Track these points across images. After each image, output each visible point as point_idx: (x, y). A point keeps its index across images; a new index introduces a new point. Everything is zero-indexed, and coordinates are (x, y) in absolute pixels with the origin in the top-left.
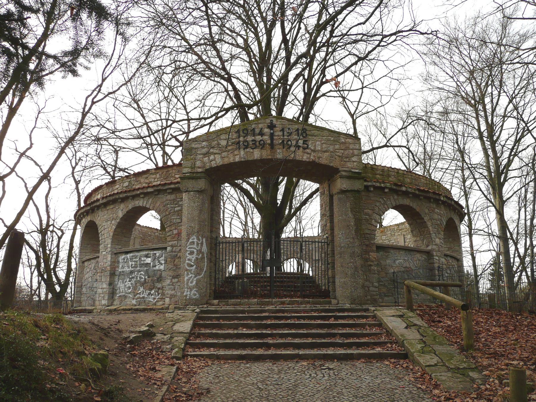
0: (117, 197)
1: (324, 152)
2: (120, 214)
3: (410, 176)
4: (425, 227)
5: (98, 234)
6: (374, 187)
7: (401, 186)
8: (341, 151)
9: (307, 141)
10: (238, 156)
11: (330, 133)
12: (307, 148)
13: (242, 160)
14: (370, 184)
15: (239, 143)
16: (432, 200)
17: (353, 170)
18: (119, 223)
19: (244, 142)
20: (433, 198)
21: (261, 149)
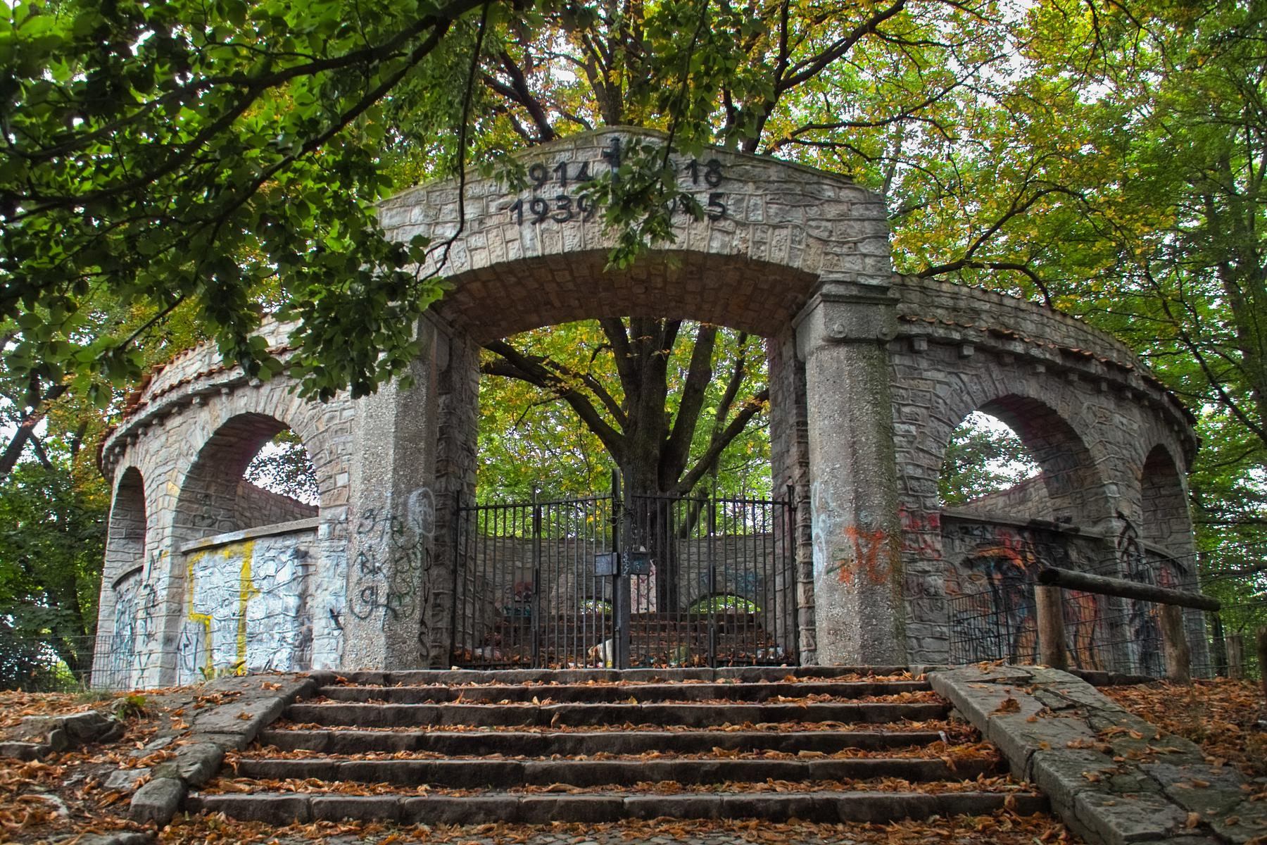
0: (190, 389)
1: (775, 227)
2: (199, 442)
3: (1035, 317)
4: (1088, 467)
5: (143, 500)
6: (931, 340)
7: (1010, 338)
8: (824, 223)
9: (720, 195)
10: (517, 244)
11: (790, 172)
12: (724, 215)
13: (529, 254)
14: (915, 330)
15: (518, 206)
16: (1104, 387)
17: (862, 281)
18: (195, 467)
19: (536, 201)
20: (1106, 379)
21: (585, 221)
